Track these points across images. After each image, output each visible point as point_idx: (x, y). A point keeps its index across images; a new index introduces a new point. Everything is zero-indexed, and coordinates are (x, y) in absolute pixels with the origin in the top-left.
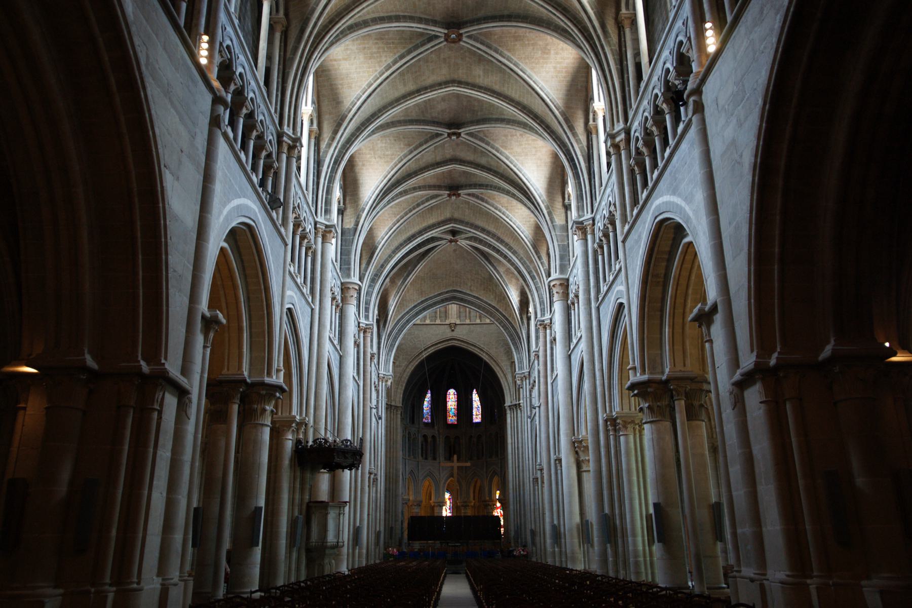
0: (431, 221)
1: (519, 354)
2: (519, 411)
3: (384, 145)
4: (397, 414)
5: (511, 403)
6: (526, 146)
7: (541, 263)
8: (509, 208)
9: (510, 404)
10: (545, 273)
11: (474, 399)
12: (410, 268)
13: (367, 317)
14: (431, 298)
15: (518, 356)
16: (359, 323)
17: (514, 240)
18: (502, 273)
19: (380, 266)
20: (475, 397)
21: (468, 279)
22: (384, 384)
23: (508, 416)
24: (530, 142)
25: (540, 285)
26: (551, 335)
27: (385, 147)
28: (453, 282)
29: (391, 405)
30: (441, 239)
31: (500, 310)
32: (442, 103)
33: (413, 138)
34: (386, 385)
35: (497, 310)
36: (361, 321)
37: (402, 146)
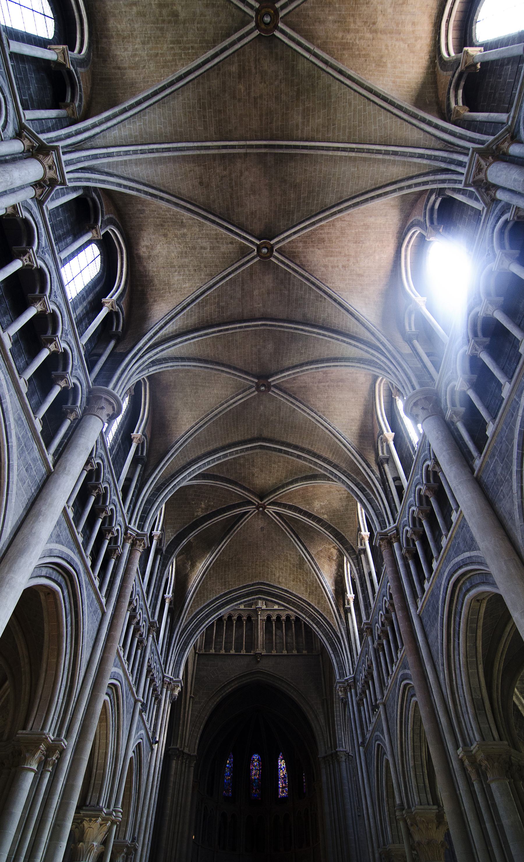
0: (236, 438)
1: (339, 656)
2: (336, 763)
3: (182, 277)
4: (189, 767)
5: (326, 753)
6: (351, 282)
7: (372, 471)
8: (326, 413)
9: (324, 755)
10: (378, 481)
11: (280, 767)
12: (214, 547)
13: (141, 527)
14: (235, 590)
15: (338, 660)
16: (127, 528)
17: (334, 453)
18: (313, 556)
19: (169, 475)
20: (282, 764)
21: (276, 568)
22: (169, 692)
23: (323, 771)
24: (355, 277)
25: (372, 496)
26: (401, 549)
27: (183, 279)
28: (260, 573)
29: (183, 753)
30: (249, 503)
31: (312, 604)
32: (252, 197)
33: (216, 266)
34: (171, 695)
35: (309, 605)
36: (131, 526)
37: (203, 277)
